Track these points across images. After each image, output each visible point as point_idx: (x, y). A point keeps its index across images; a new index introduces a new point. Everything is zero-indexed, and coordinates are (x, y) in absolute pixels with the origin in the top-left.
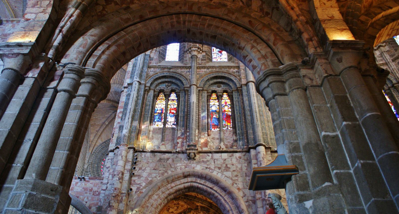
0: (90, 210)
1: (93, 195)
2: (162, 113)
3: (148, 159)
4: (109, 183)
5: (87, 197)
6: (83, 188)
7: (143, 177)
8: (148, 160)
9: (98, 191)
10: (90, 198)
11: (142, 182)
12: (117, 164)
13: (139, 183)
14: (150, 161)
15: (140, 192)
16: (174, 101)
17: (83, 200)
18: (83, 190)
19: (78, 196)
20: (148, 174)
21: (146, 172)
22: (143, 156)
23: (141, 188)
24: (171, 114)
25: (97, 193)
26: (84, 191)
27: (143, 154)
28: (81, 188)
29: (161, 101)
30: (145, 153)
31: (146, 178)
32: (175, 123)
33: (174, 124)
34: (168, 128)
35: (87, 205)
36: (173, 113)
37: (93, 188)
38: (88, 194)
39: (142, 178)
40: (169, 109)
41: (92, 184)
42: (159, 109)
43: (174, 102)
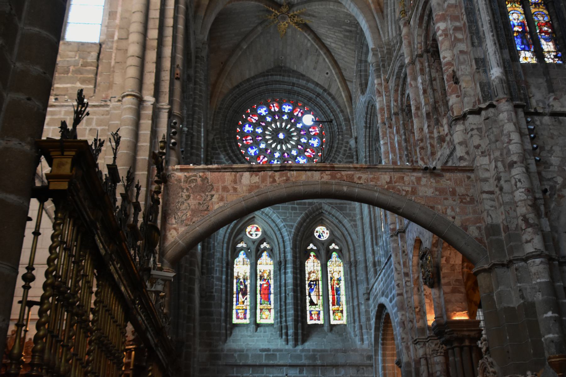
0: (468, 233)
1: (461, 202)
2: (524, 31)
3: (550, 129)
4: (502, 179)
5: (450, 207)
6: (436, 189)
7: (552, 165)
8: (551, 131)
9: (468, 196)
10: (458, 210)
11: (555, 175)
12: (511, 140)
13: (550, 177)
14: (556, 133)
15: (559, 195)
16: (539, 6)
17: (446, 214)
18: (437, 193)
19: (431, 204)
20: (560, 159)
21: (554, 154)
22: (538, 123)
23: (558, 186)
24: (543, 34)
25: (468, 199)
26: (440, 195)
27: (536, 118)
28: (432, 190)
29: (514, 6)
30: (540, 118)
31: (559, 166)
32: (560, 54)
33: (556, 57)
34: (550, 64)
35: (458, 222)
36: (546, 32)
37: (457, 189)
38: (450, 201)
39: (552, 168)
40: (536, 23)
41: (450, 179)
42: (516, 24)
43: (541, 10)
